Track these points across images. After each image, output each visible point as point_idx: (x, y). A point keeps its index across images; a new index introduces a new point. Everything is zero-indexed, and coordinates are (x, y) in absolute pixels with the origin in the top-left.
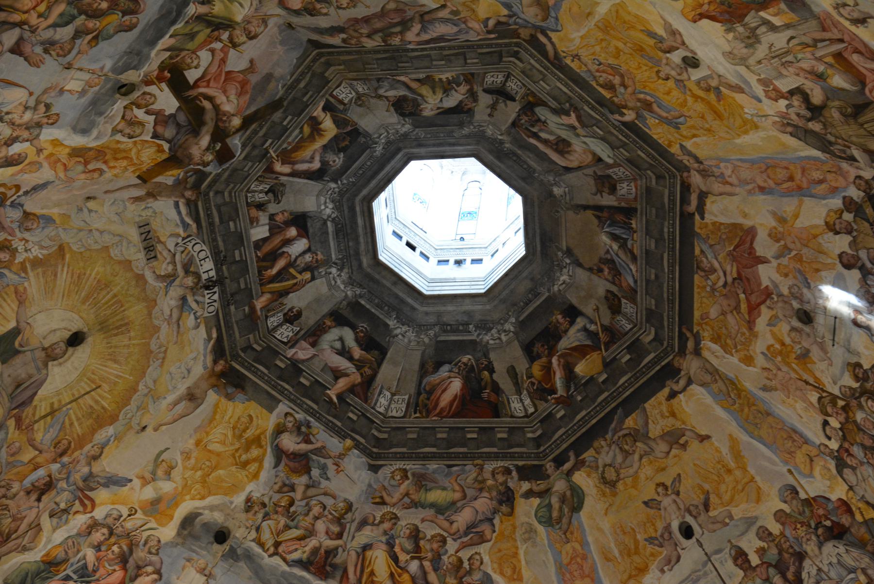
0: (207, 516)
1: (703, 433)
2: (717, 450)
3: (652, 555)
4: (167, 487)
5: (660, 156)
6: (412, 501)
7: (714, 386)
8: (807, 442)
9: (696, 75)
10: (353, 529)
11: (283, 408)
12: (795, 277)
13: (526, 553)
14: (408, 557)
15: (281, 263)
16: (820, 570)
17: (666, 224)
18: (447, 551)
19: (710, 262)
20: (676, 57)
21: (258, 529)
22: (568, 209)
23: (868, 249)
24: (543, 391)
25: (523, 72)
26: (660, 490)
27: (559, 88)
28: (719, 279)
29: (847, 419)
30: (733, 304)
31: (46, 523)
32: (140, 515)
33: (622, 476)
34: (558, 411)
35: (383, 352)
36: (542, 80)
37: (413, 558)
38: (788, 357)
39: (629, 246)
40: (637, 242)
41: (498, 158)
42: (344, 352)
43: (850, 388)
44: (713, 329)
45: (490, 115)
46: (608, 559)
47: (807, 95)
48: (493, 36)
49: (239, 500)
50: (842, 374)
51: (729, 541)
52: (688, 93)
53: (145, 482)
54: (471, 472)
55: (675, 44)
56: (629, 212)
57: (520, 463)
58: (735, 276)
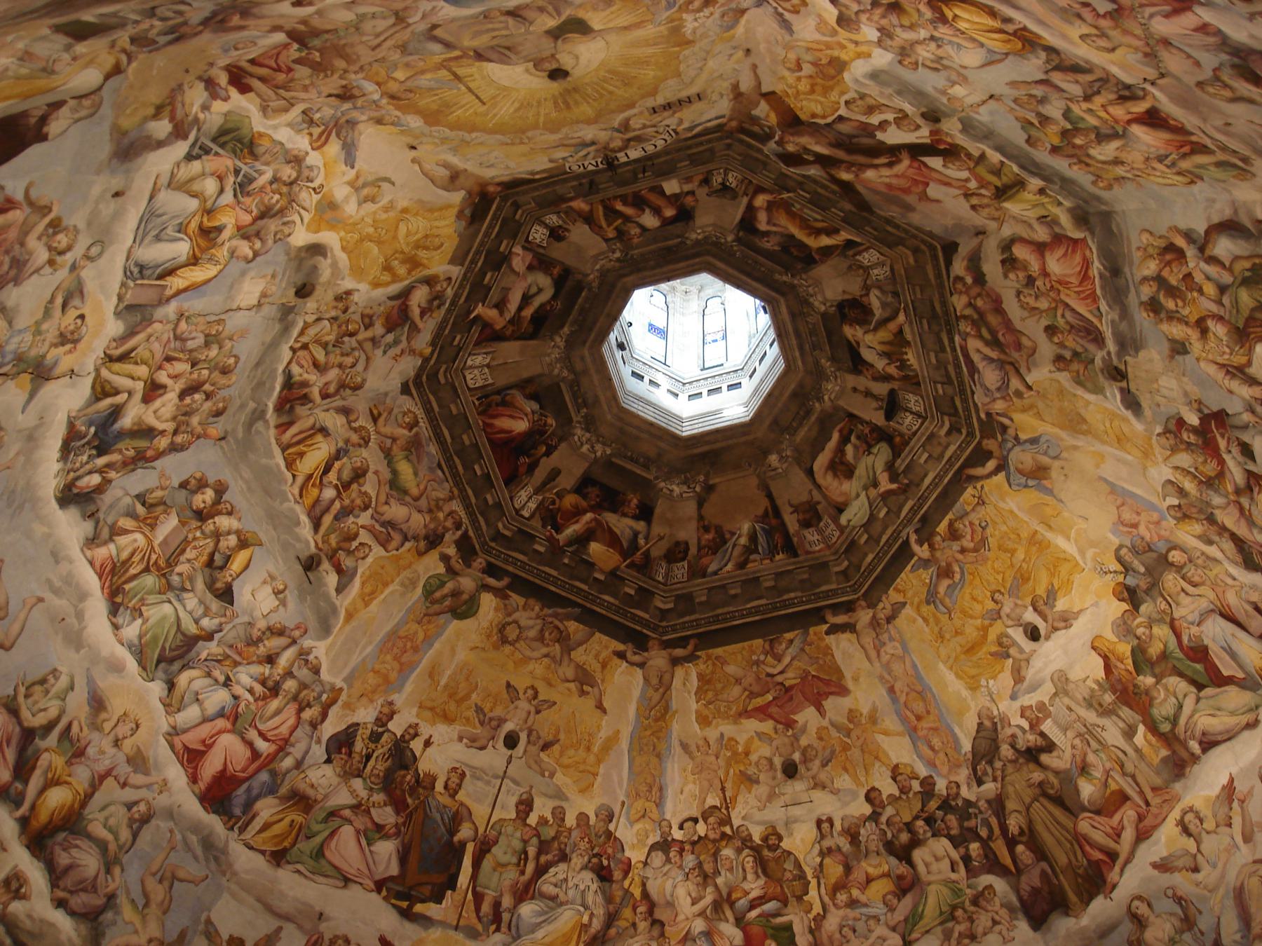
0: (325, 266)
1: (605, 704)
2: (599, 728)
3: (468, 719)
4: (351, 208)
5: (876, 578)
6: (390, 449)
7: (651, 692)
8: (659, 804)
9: (1018, 635)
10: (334, 404)
11: (456, 271)
12: (824, 748)
13: (392, 593)
14: (335, 482)
15: (629, 211)
16: (566, 880)
17: (799, 594)
18: (358, 517)
19: (784, 652)
20: (1030, 616)
21: (319, 319)
22: (758, 476)
23: (898, 814)
24: (552, 517)
25: (932, 436)
26: (530, 692)
27: (926, 475)
28: (774, 667)
29: (714, 841)
30: (756, 688)
31: (295, 112)
32: (316, 198)
33: (517, 645)
34: (541, 544)
35: (532, 336)
36: (930, 456)
37: (336, 487)
38: (737, 762)
39: (752, 557)
40: (759, 565)
41: (795, 395)
42: (526, 299)
43: (750, 835)
44: (713, 673)
45: (855, 390)
46: (431, 675)
47: (1050, 752)
48: (983, 416)
49: (348, 284)
50: (759, 823)
51: (531, 787)
52: (987, 622)
53: (354, 185)
54: (441, 492)
55: (1050, 618)
56: (791, 549)
57: (471, 533)
58: (787, 684)
